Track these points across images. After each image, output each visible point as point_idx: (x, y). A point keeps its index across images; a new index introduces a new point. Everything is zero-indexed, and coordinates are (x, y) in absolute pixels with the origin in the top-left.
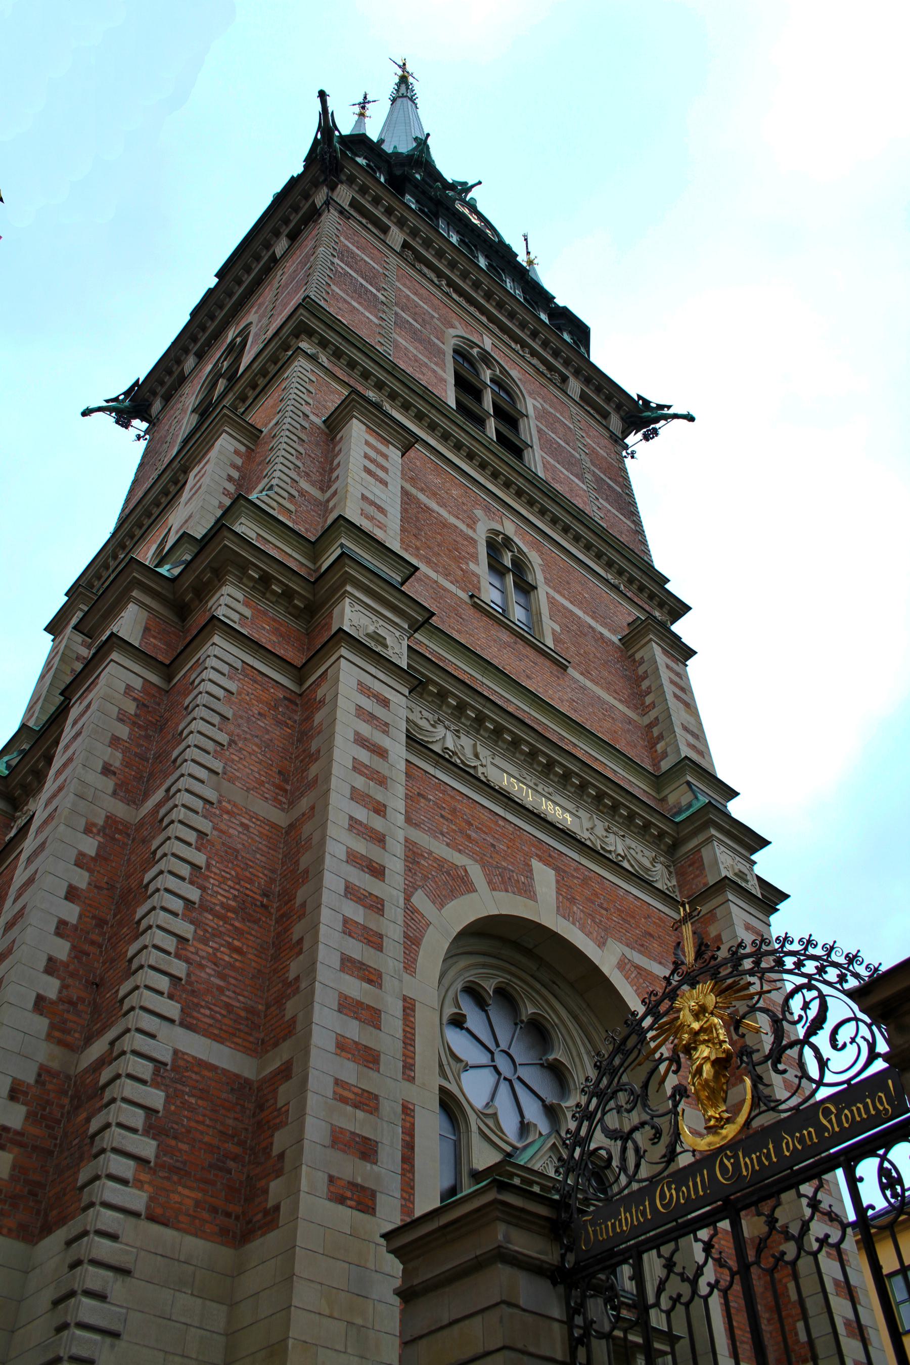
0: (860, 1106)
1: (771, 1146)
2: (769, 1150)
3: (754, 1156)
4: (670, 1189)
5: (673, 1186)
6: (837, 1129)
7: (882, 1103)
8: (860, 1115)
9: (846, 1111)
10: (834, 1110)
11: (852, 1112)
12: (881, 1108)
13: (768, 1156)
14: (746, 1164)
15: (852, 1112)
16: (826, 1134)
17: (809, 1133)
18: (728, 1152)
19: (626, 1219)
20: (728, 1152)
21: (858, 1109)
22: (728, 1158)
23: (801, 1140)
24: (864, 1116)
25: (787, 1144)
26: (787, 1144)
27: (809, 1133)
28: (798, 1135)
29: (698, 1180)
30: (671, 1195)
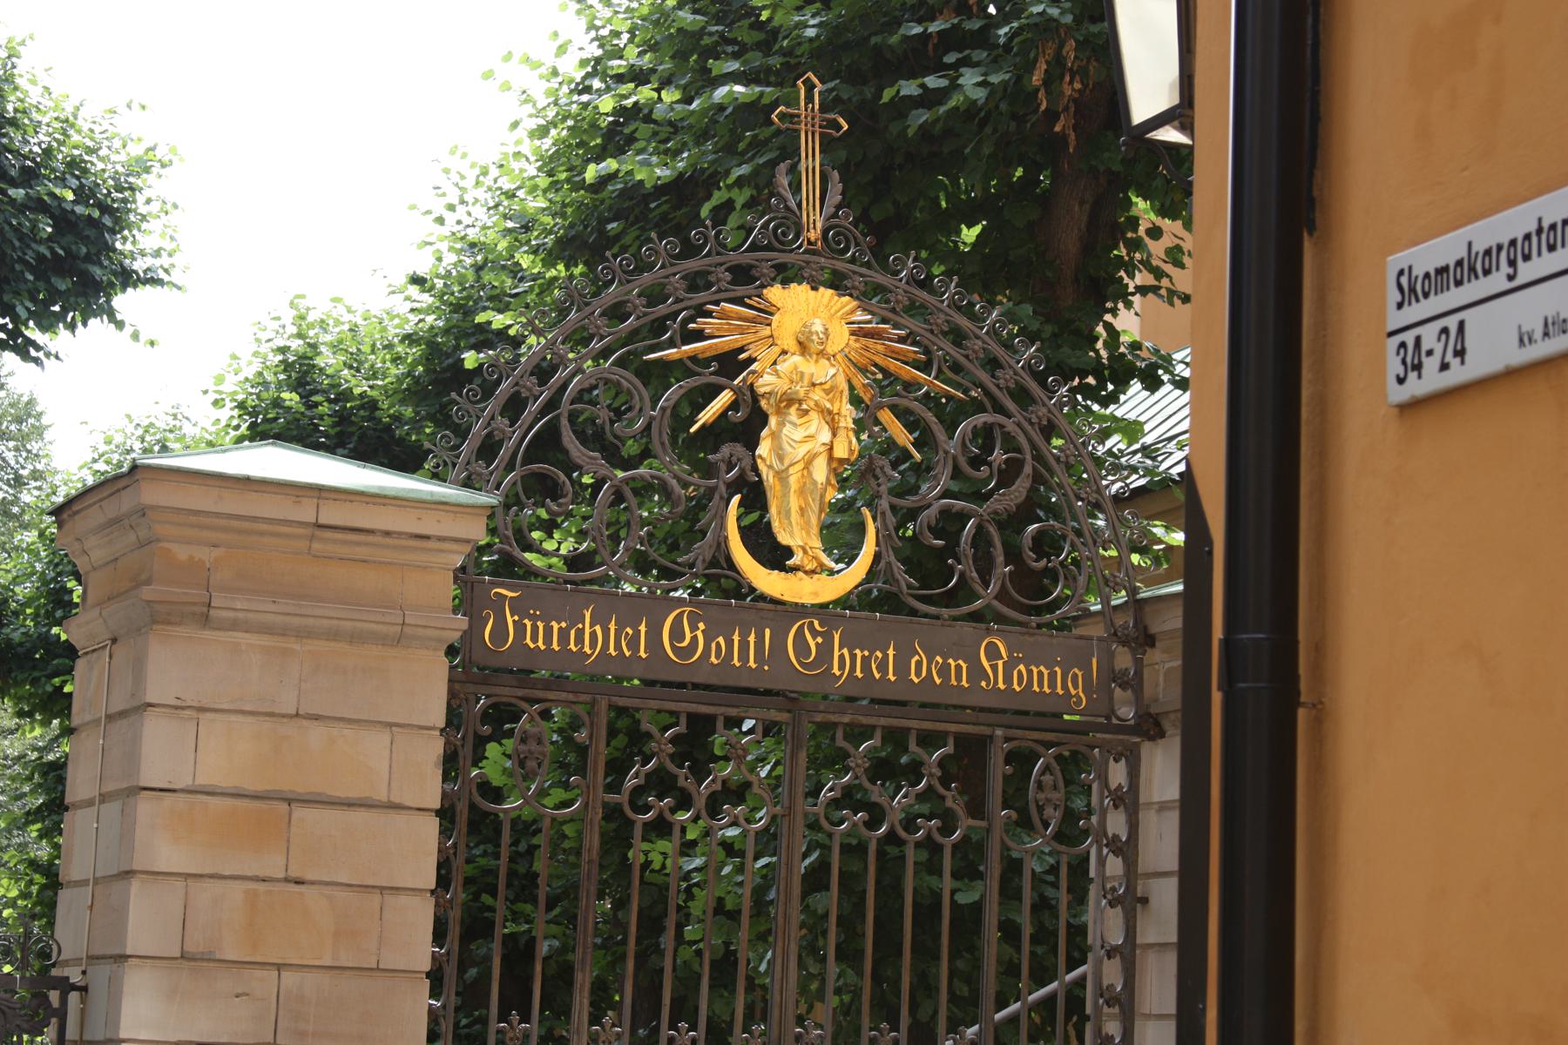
0: (1046, 672)
1: (891, 652)
2: (886, 656)
3: (858, 651)
4: (694, 628)
5: (701, 626)
6: (1001, 686)
7: (1076, 686)
8: (1041, 685)
9: (1022, 667)
10: (1005, 656)
11: (1030, 672)
12: (1073, 692)
13: (883, 667)
14: (842, 657)
15: (1030, 672)
16: (983, 684)
17: (958, 667)
18: (816, 623)
19: (593, 635)
20: (816, 623)
21: (1040, 674)
22: (815, 633)
23: (944, 671)
24: (1046, 689)
25: (919, 664)
26: (919, 664)
27: (958, 667)
28: (939, 659)
29: (752, 639)
30: (694, 639)
